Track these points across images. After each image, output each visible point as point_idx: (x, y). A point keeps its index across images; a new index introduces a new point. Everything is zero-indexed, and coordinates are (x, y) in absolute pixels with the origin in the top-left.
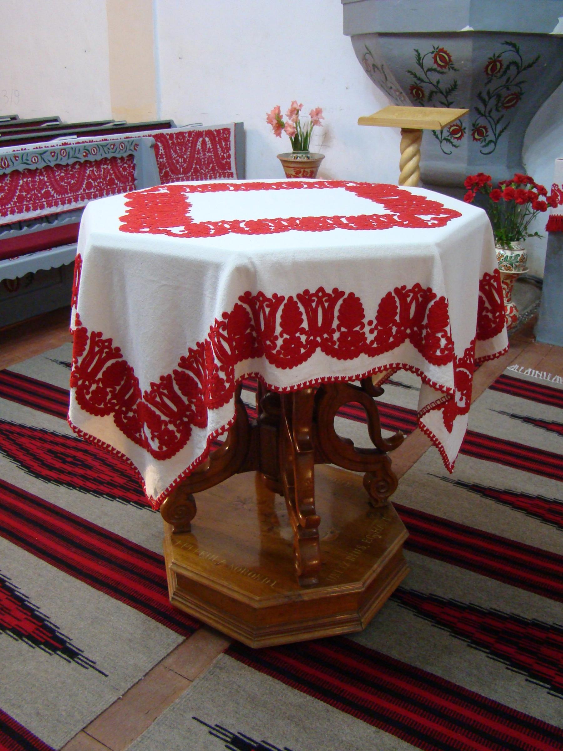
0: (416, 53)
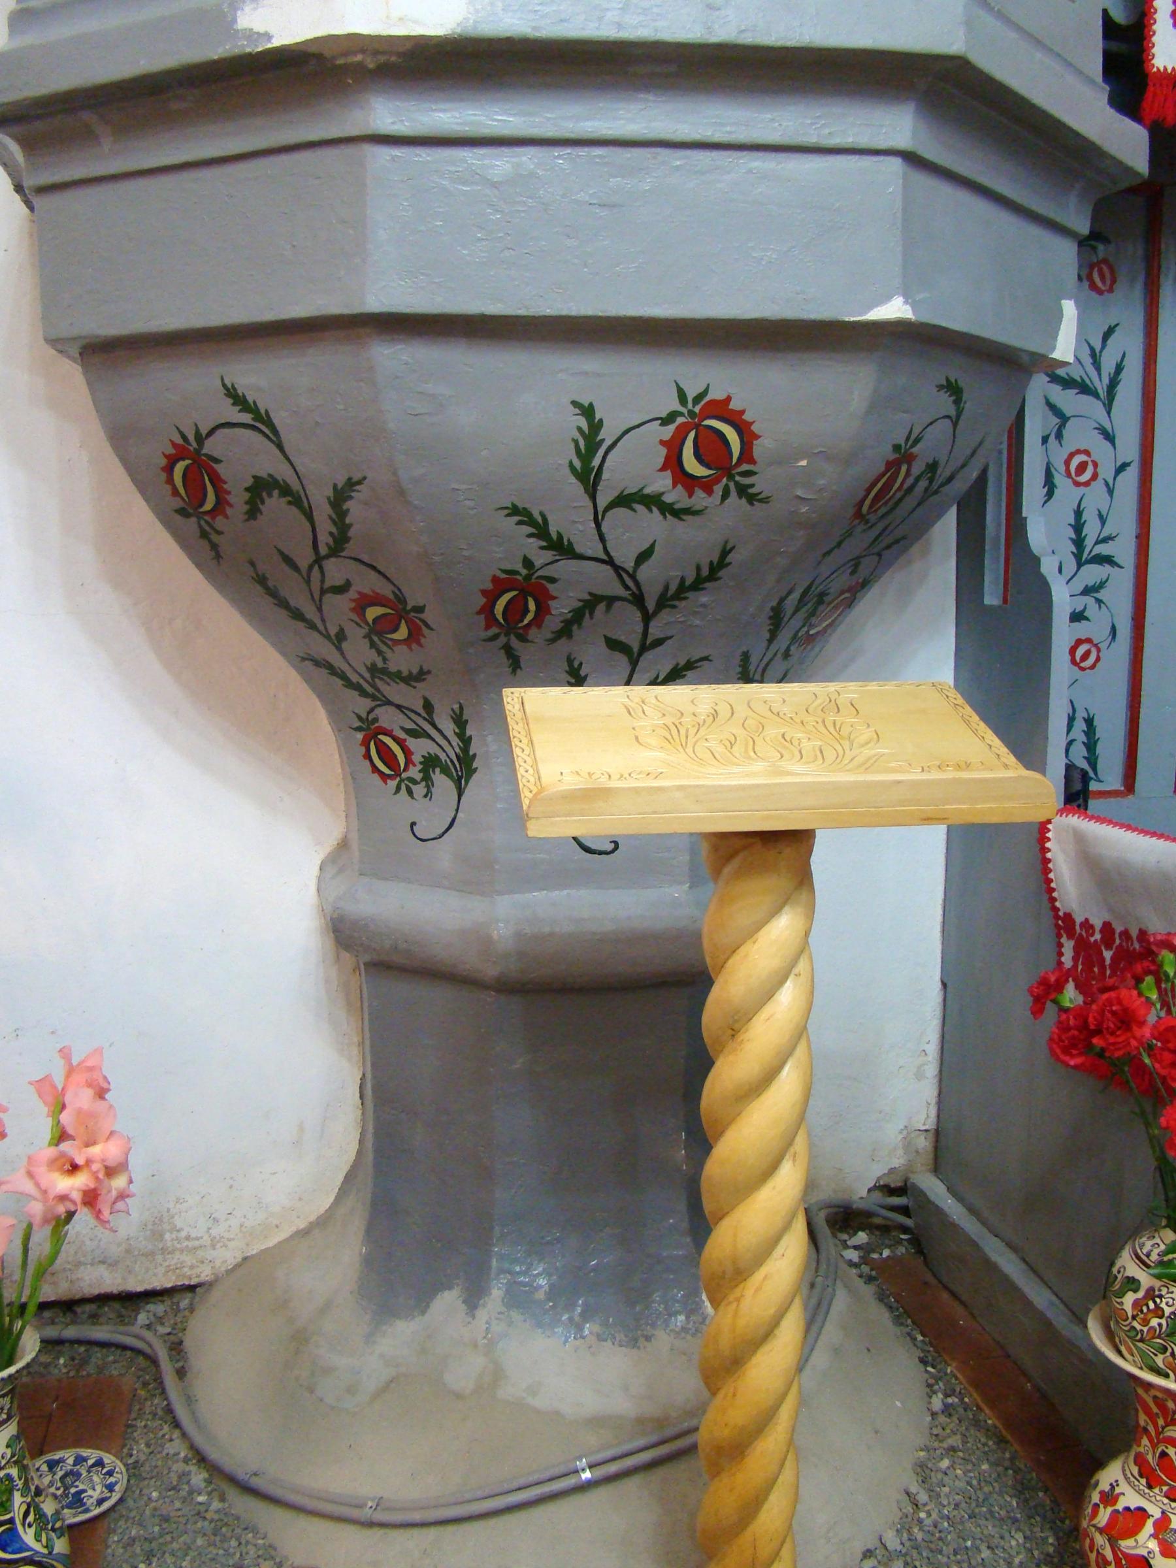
0: (583, 423)
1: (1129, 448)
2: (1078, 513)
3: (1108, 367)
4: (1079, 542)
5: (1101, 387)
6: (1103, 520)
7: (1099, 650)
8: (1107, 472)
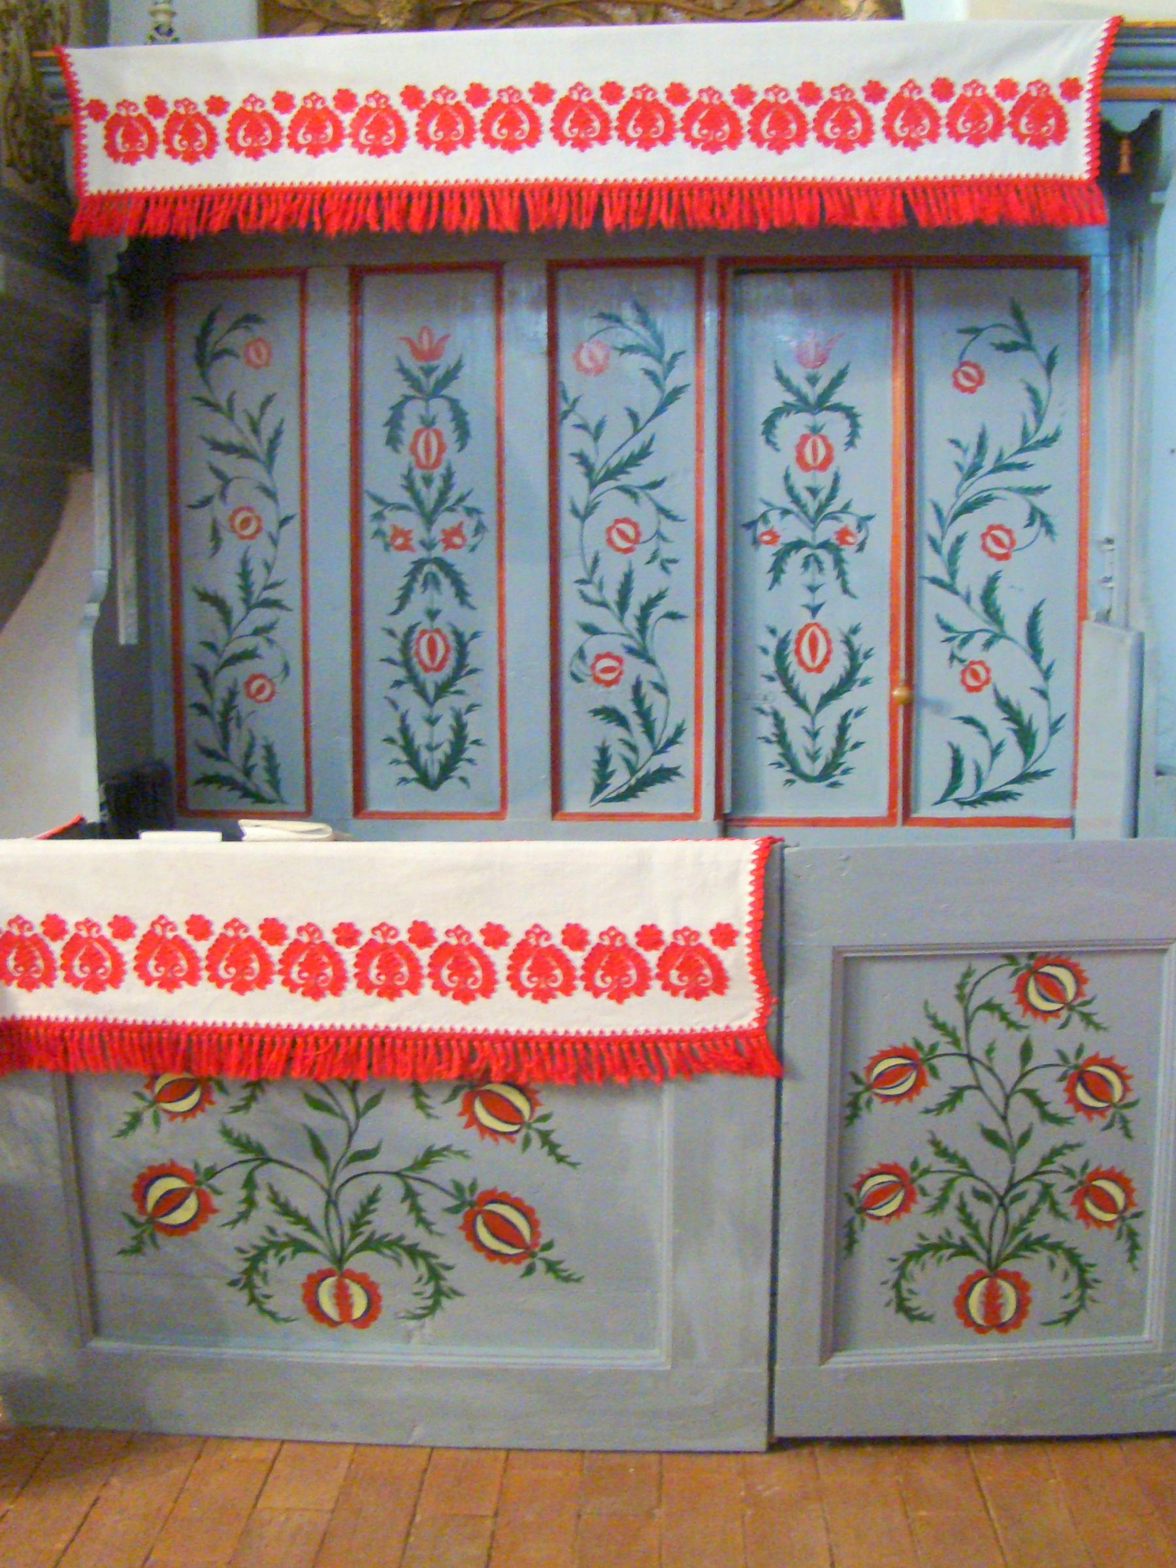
1: (290, 506)
2: (245, 563)
3: (267, 431)
4: (246, 588)
5: (261, 449)
6: (268, 567)
7: (273, 685)
8: (271, 525)
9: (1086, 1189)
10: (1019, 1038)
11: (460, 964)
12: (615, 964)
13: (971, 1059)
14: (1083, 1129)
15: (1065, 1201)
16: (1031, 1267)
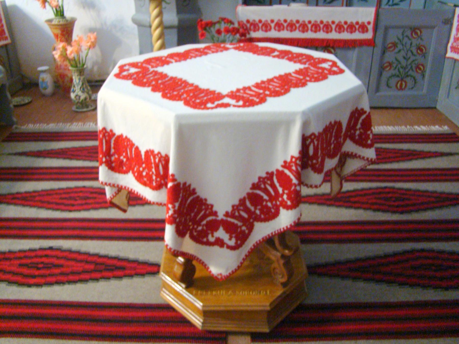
9: (418, 67)
10: (410, 42)
11: (327, 28)
12: (351, 28)
13: (403, 45)
14: (418, 57)
15: (414, 69)
16: (408, 80)
